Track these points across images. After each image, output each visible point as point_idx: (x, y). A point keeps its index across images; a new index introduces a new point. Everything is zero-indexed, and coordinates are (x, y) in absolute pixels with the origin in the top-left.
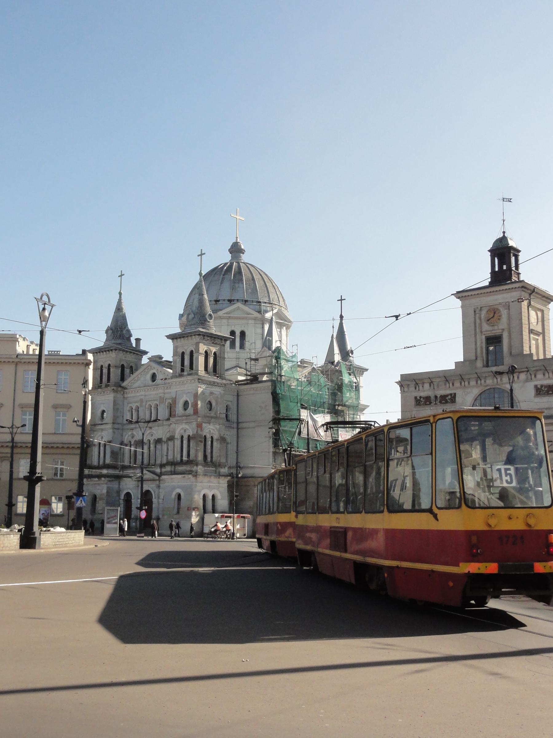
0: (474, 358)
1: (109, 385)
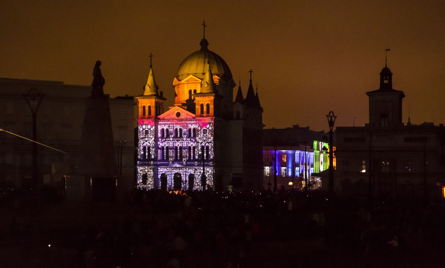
1: (150, 117)
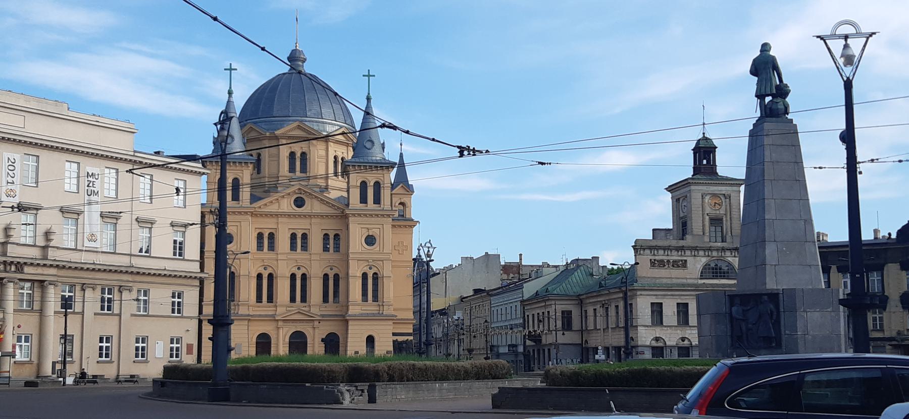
0: (702, 233)
